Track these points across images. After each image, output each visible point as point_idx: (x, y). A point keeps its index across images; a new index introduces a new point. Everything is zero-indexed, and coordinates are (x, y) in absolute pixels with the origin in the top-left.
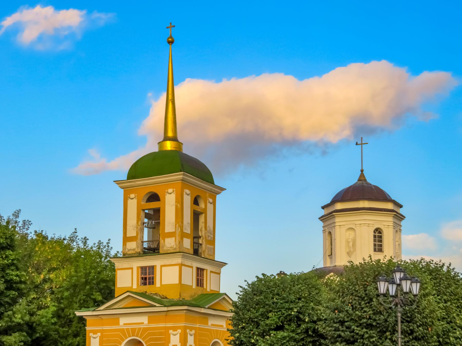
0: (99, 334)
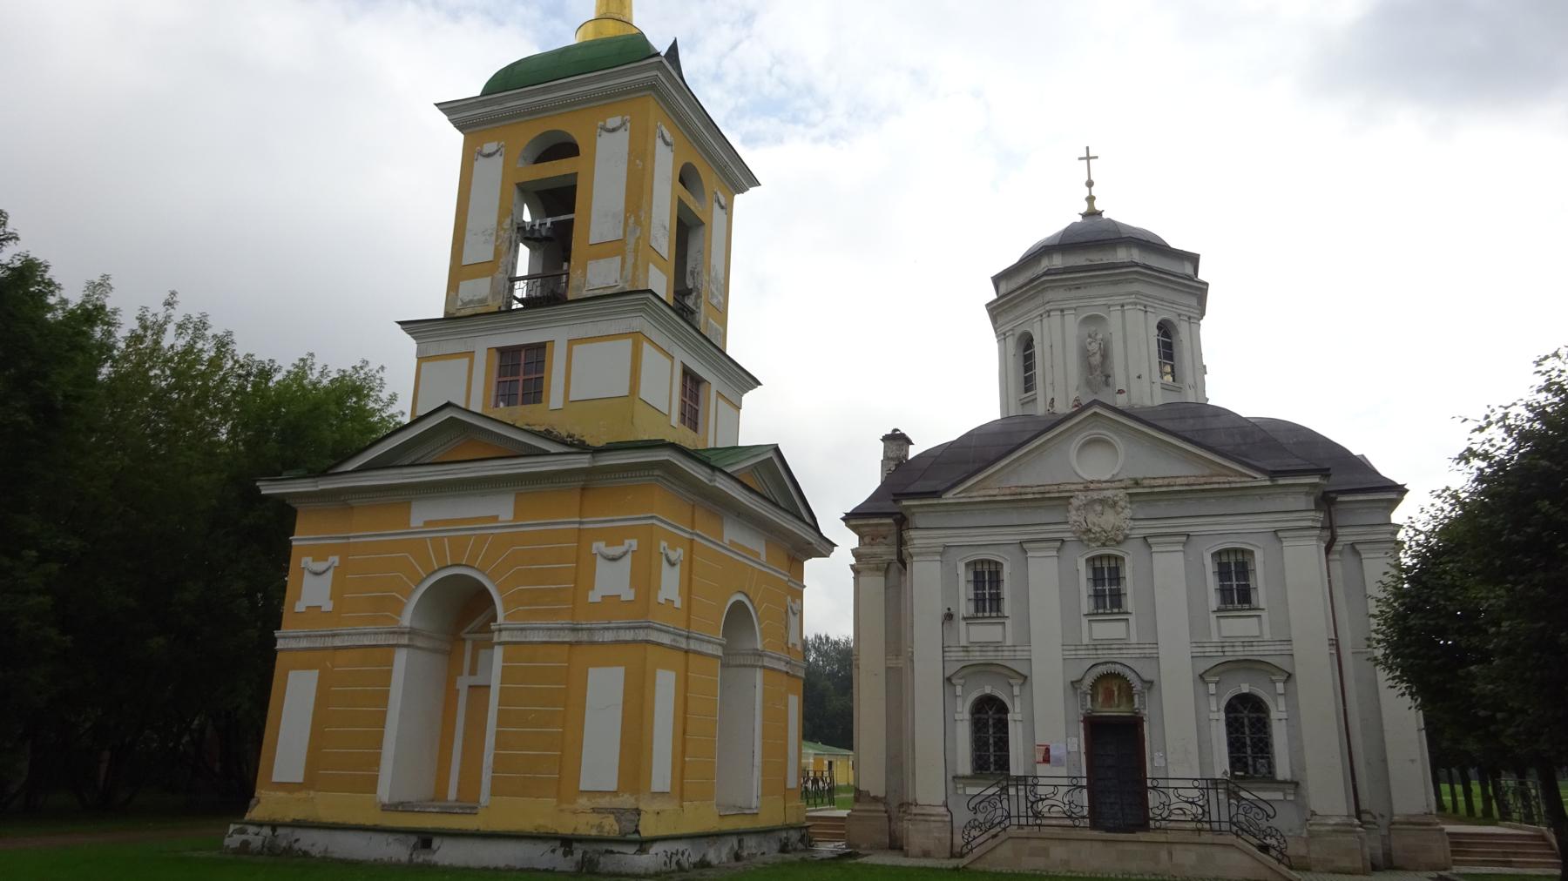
0: (335, 560)
